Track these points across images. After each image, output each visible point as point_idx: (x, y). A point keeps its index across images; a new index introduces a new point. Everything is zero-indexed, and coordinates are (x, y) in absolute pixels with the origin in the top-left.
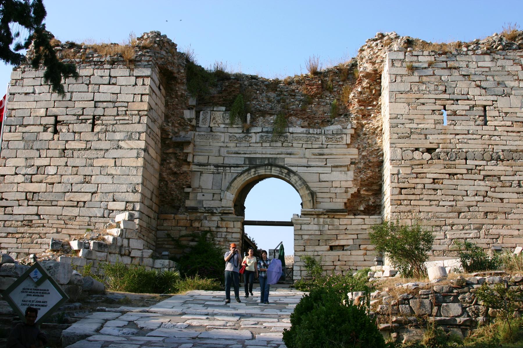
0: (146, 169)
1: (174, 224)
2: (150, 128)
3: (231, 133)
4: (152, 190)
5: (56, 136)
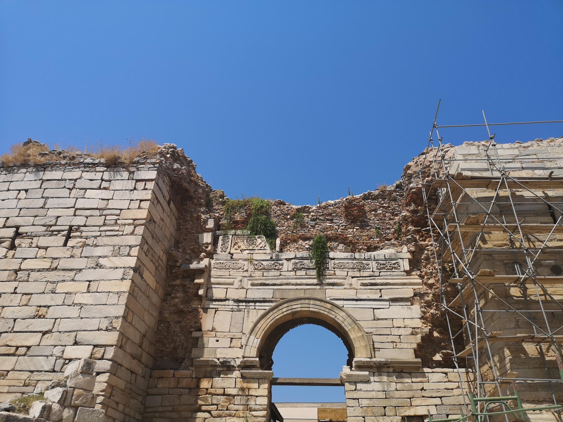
0: (135, 298)
1: (172, 386)
2: (147, 243)
4: (143, 331)
5: (11, 253)
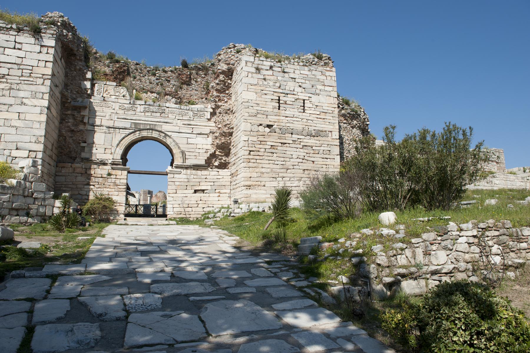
1: (71, 172)
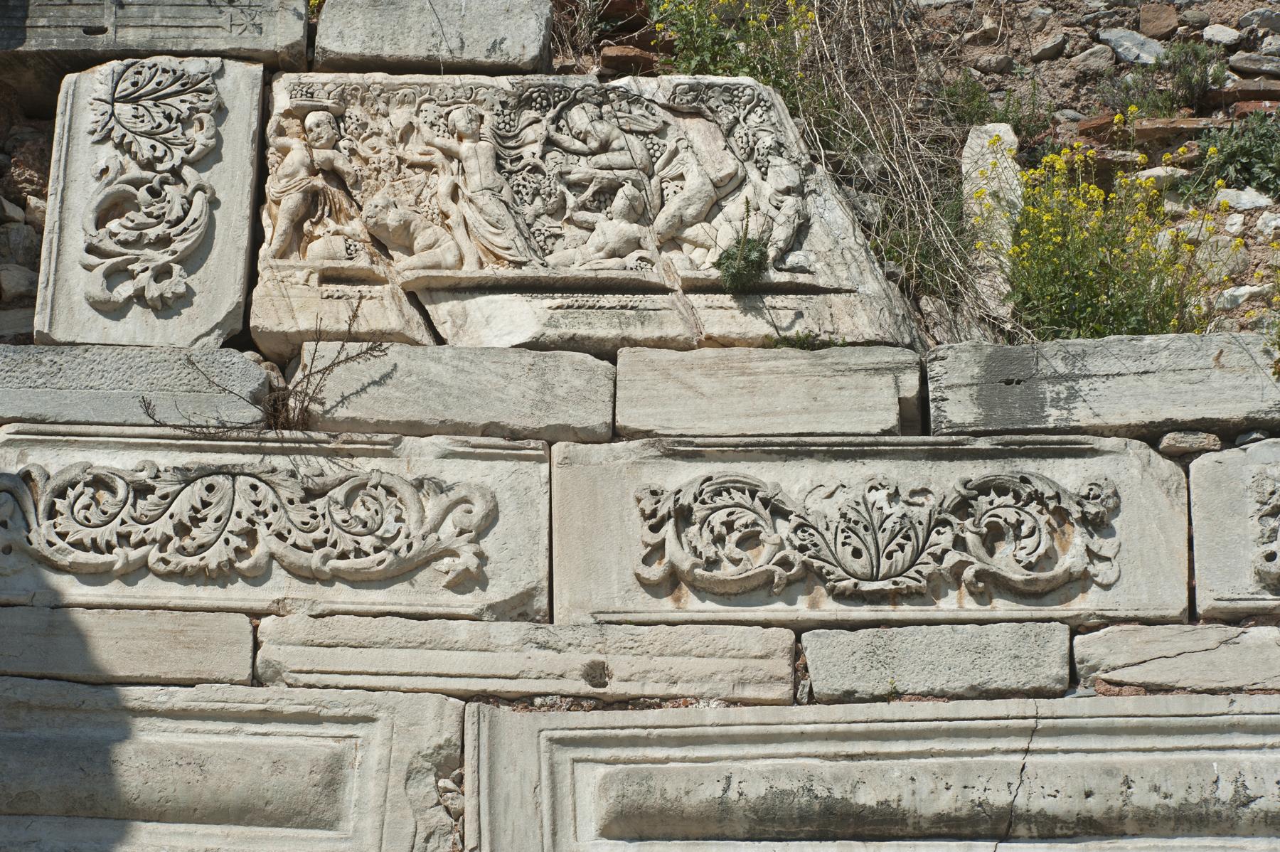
3: (683, 449)
